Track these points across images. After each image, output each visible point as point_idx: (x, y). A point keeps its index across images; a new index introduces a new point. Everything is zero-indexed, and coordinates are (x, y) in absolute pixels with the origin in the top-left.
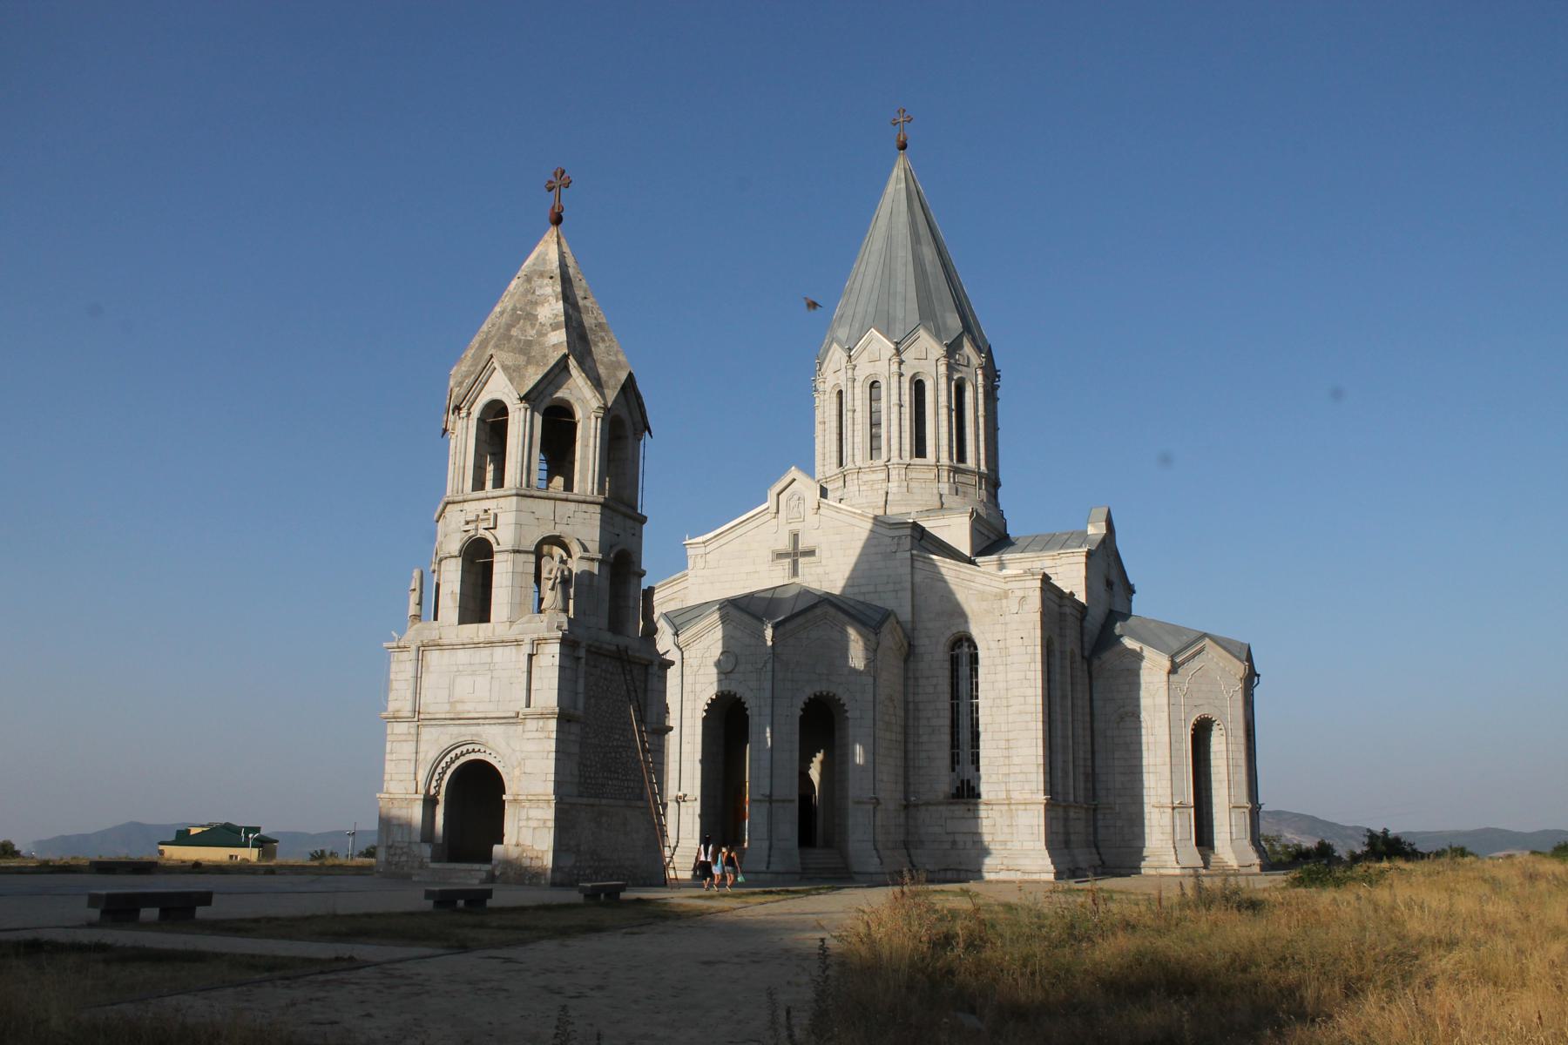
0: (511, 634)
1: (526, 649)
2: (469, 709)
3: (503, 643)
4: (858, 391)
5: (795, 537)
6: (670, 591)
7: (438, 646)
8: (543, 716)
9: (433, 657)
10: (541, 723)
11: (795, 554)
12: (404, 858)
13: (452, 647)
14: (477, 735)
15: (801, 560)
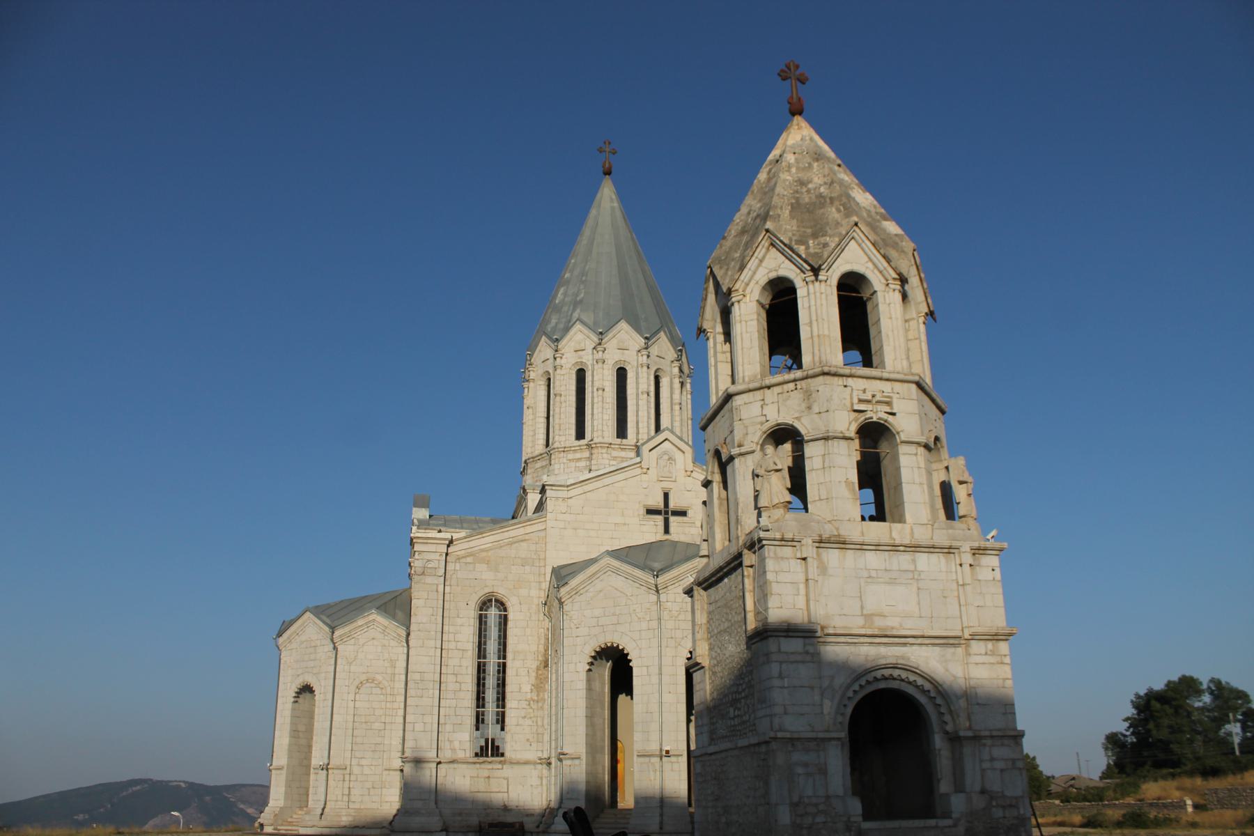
0: (941, 538)
1: (968, 558)
2: (891, 624)
3: (932, 548)
4: (606, 372)
5: (666, 496)
6: (522, 531)
7: (842, 543)
8: (995, 637)
9: (832, 556)
10: (990, 645)
11: (666, 513)
12: (819, 819)
13: (861, 547)
14: (903, 658)
15: (672, 519)
